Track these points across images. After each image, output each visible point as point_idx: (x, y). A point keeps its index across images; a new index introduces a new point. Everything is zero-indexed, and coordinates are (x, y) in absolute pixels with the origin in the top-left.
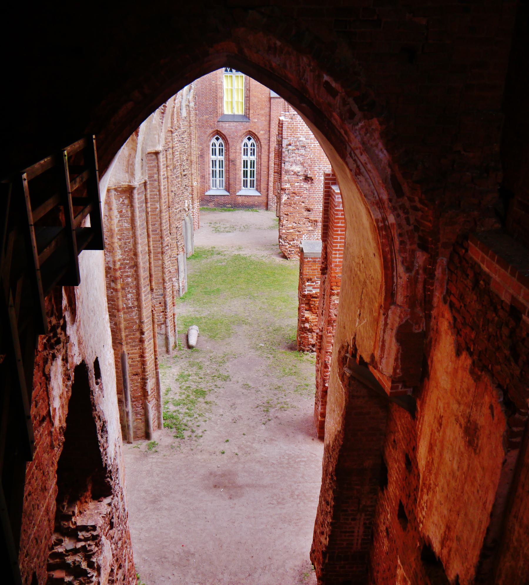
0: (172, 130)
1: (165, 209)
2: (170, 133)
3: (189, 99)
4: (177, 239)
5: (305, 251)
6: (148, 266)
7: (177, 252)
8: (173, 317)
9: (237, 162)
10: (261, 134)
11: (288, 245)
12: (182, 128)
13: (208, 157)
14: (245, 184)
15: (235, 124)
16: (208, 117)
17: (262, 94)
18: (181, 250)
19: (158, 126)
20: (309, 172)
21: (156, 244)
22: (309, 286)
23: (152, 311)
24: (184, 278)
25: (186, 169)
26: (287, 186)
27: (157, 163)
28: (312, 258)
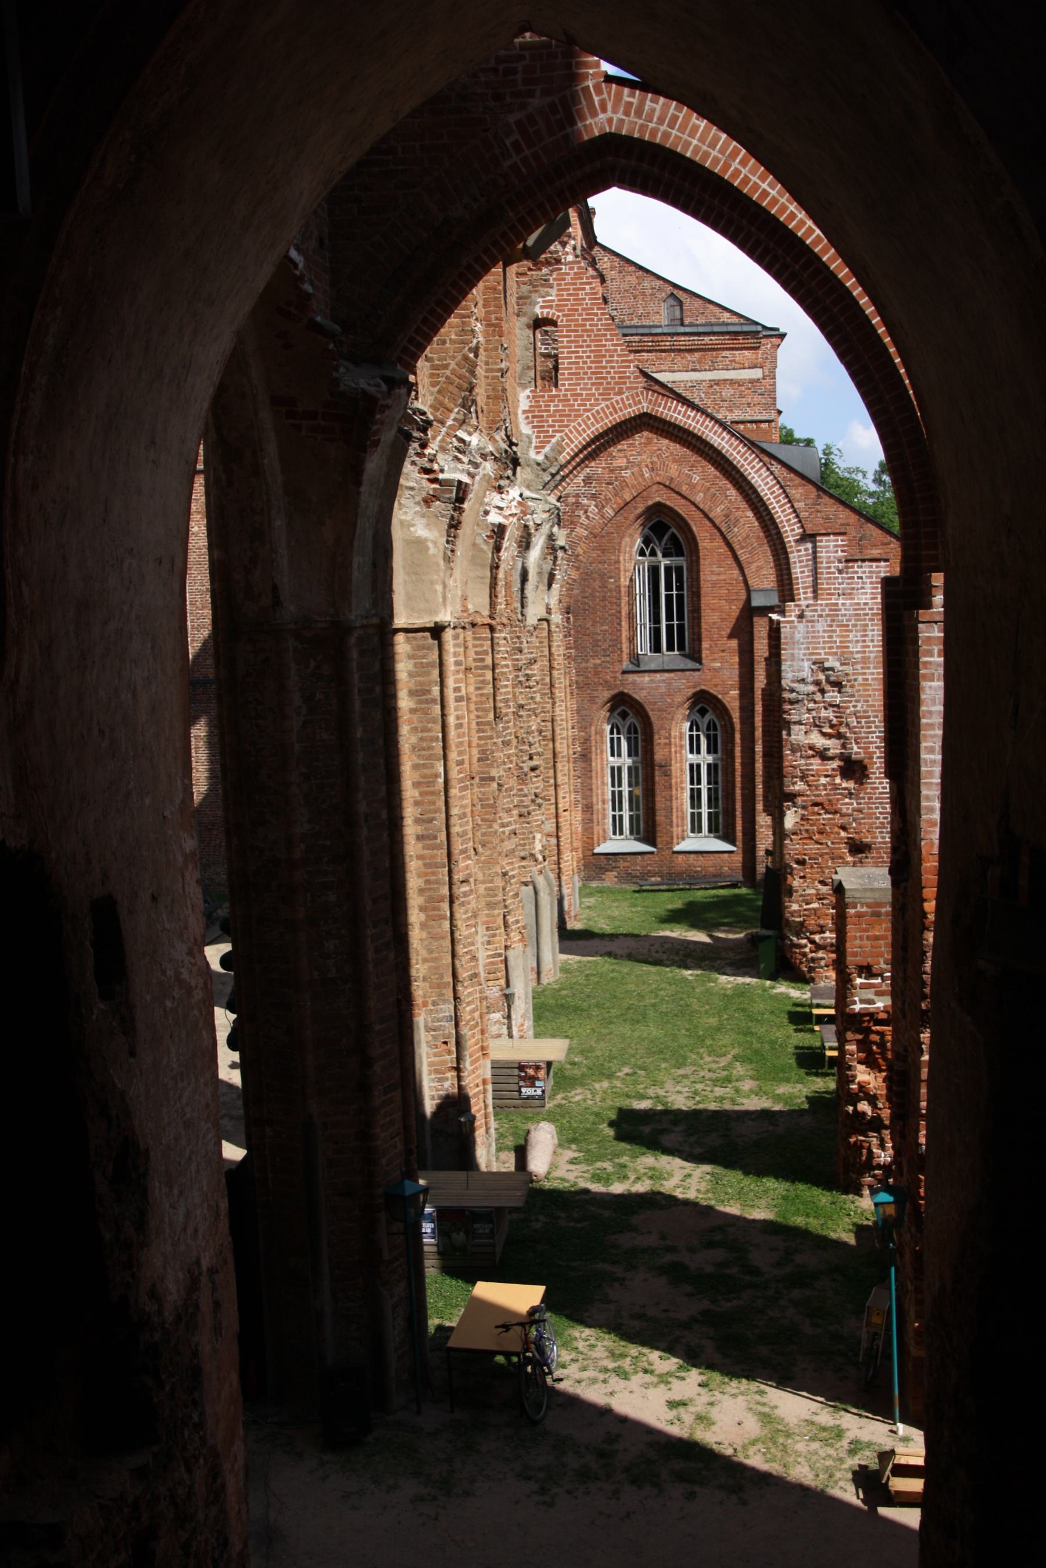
0: (493, 622)
1: (461, 780)
2: (488, 631)
3: (547, 605)
4: (506, 907)
5: (846, 885)
6: (387, 864)
7: (506, 940)
8: (481, 1088)
9: (673, 768)
10: (732, 699)
11: (809, 945)
12: (526, 651)
13: (602, 759)
14: (696, 827)
15: (666, 675)
16: (598, 662)
17: (730, 602)
18: (515, 936)
19: (442, 562)
20: (855, 749)
21: (434, 874)
22: (863, 986)
23: (399, 1001)
24: (524, 1016)
25: (538, 754)
26: (799, 786)
27: (440, 656)
28: (868, 905)
